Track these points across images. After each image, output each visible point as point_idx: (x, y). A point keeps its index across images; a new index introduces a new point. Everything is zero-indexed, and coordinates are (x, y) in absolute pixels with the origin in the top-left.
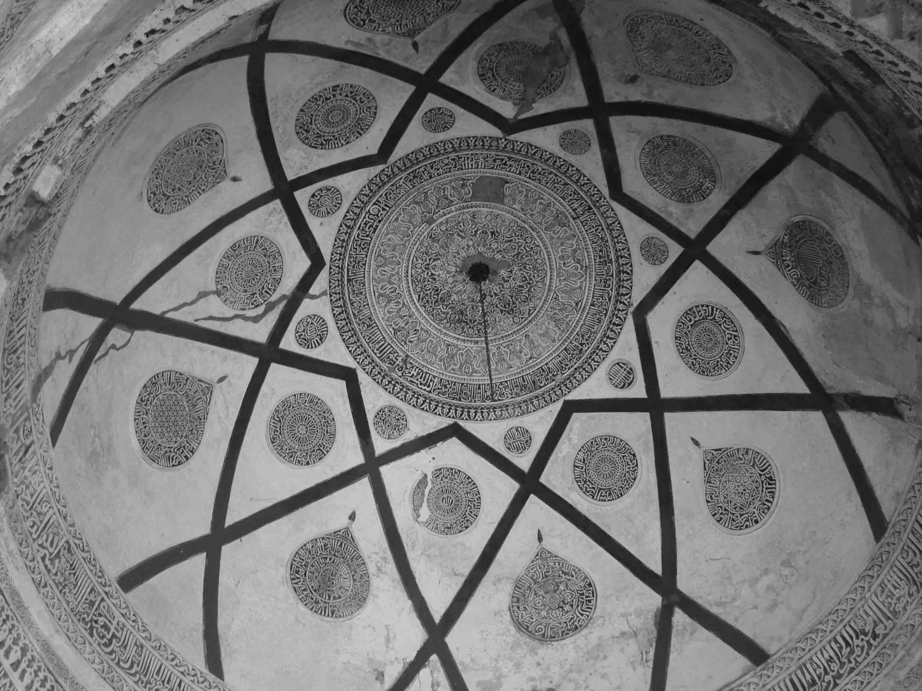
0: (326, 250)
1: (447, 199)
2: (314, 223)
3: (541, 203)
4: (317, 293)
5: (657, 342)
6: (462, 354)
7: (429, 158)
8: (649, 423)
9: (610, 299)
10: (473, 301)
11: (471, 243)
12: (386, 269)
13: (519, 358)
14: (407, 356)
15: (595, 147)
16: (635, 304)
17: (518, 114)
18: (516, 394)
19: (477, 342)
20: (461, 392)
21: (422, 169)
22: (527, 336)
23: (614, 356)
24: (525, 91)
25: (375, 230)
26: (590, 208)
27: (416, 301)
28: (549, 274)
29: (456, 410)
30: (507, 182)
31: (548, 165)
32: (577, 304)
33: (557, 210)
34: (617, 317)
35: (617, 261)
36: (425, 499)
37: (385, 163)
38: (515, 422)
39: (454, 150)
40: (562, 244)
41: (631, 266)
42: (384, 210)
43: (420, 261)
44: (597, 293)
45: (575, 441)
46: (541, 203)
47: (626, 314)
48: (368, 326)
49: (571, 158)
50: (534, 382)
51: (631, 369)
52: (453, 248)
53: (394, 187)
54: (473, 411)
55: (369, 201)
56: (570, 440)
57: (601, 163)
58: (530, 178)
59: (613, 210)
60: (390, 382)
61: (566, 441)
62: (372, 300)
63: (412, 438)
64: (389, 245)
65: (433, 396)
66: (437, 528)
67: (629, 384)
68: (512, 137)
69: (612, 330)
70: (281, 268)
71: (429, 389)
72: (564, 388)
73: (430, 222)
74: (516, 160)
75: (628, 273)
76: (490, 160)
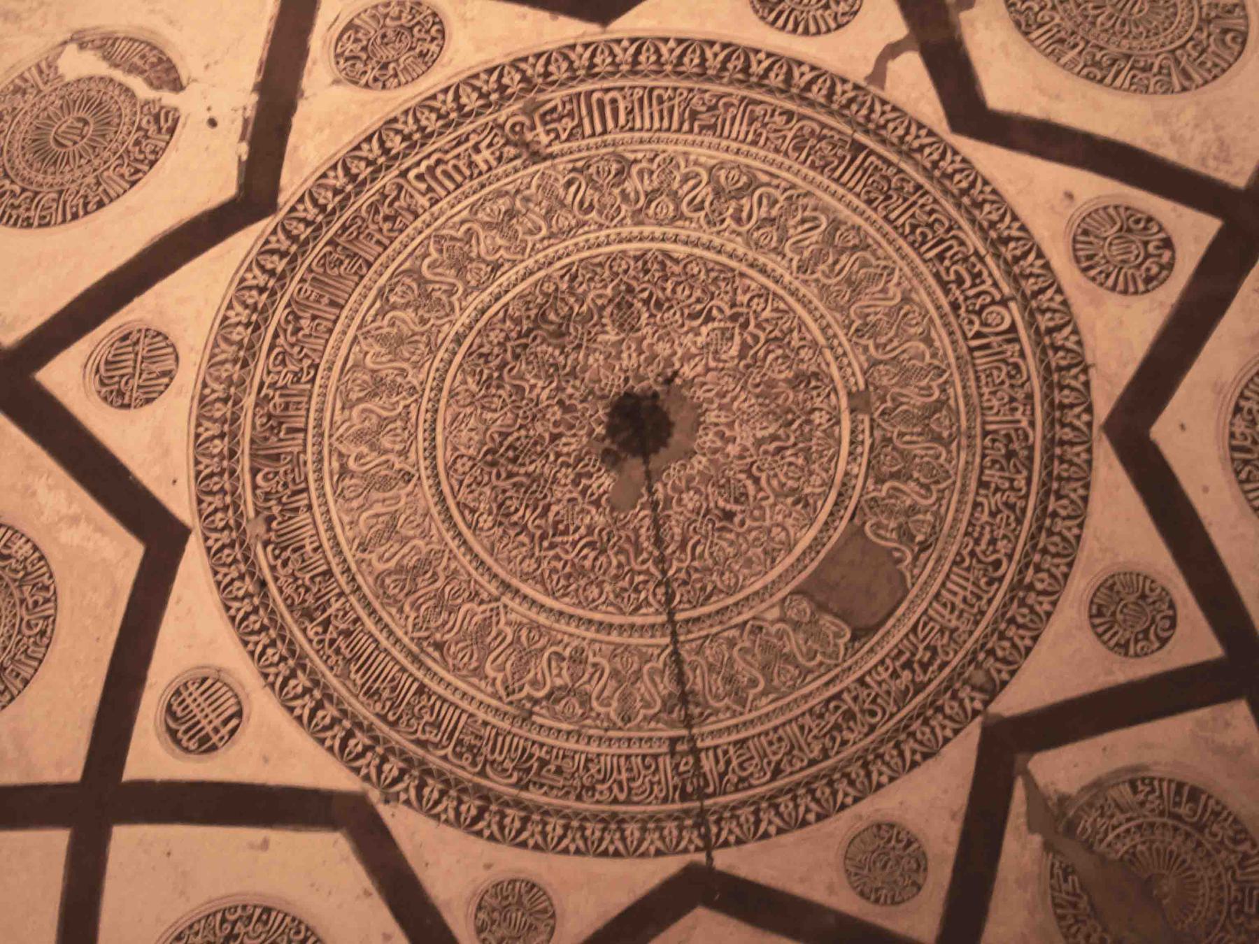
0: (993, 162)
1: (895, 476)
2: (1092, 187)
3: (753, 683)
4: (893, 66)
5: (265, 845)
6: (450, 293)
7: (1039, 519)
8: (51, 775)
9: (422, 744)
10: (573, 374)
11: (732, 449)
12: (815, 235)
13: (359, 437)
14: (536, 156)
15: (847, 902)
16: (385, 811)
17: (1031, 784)
18: (268, 399)
19: (459, 340)
20: (349, 255)
21: (1020, 482)
22: (407, 477)
23: (263, 707)
24: (1089, 847)
25: (944, 286)
26: (685, 797)
27: (668, 246)
28: (549, 602)
29: (308, 223)
30: (854, 638)
31: (850, 761)
32: (439, 646)
33: (716, 712)
34: (367, 749)
35: (518, 804)
36: (118, 75)
37: (1108, 427)
38: (188, 376)
39: (1018, 584)
40: (615, 674)
41: (492, 838)
42: (978, 335)
43: (767, 314)
44: (449, 715)
45: (71, 536)
46: (753, 683)
47: (367, 778)
48: (694, 115)
49: (841, 825)
50: (277, 458)
51: (214, 748)
52: (745, 402)
53: (1020, 395)
54: (281, 266)
55: (1031, 323)
56: (74, 520)
57: (798, 890)
58: (837, 696)
59: (659, 853)
60: (502, 88)
61: (75, 509)
62: (758, 160)
63: (307, 83)
64: (873, 279)
65: (387, 179)
66: (17, 90)
67: (173, 733)
68: (973, 731)
69: (335, 721)
70: (1055, 57)
71: (411, 175)
72: (225, 537)
73: (859, 402)
74: (903, 697)
75: (475, 820)
76: (941, 642)
